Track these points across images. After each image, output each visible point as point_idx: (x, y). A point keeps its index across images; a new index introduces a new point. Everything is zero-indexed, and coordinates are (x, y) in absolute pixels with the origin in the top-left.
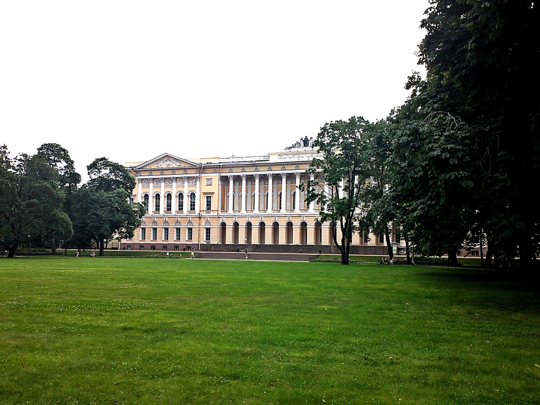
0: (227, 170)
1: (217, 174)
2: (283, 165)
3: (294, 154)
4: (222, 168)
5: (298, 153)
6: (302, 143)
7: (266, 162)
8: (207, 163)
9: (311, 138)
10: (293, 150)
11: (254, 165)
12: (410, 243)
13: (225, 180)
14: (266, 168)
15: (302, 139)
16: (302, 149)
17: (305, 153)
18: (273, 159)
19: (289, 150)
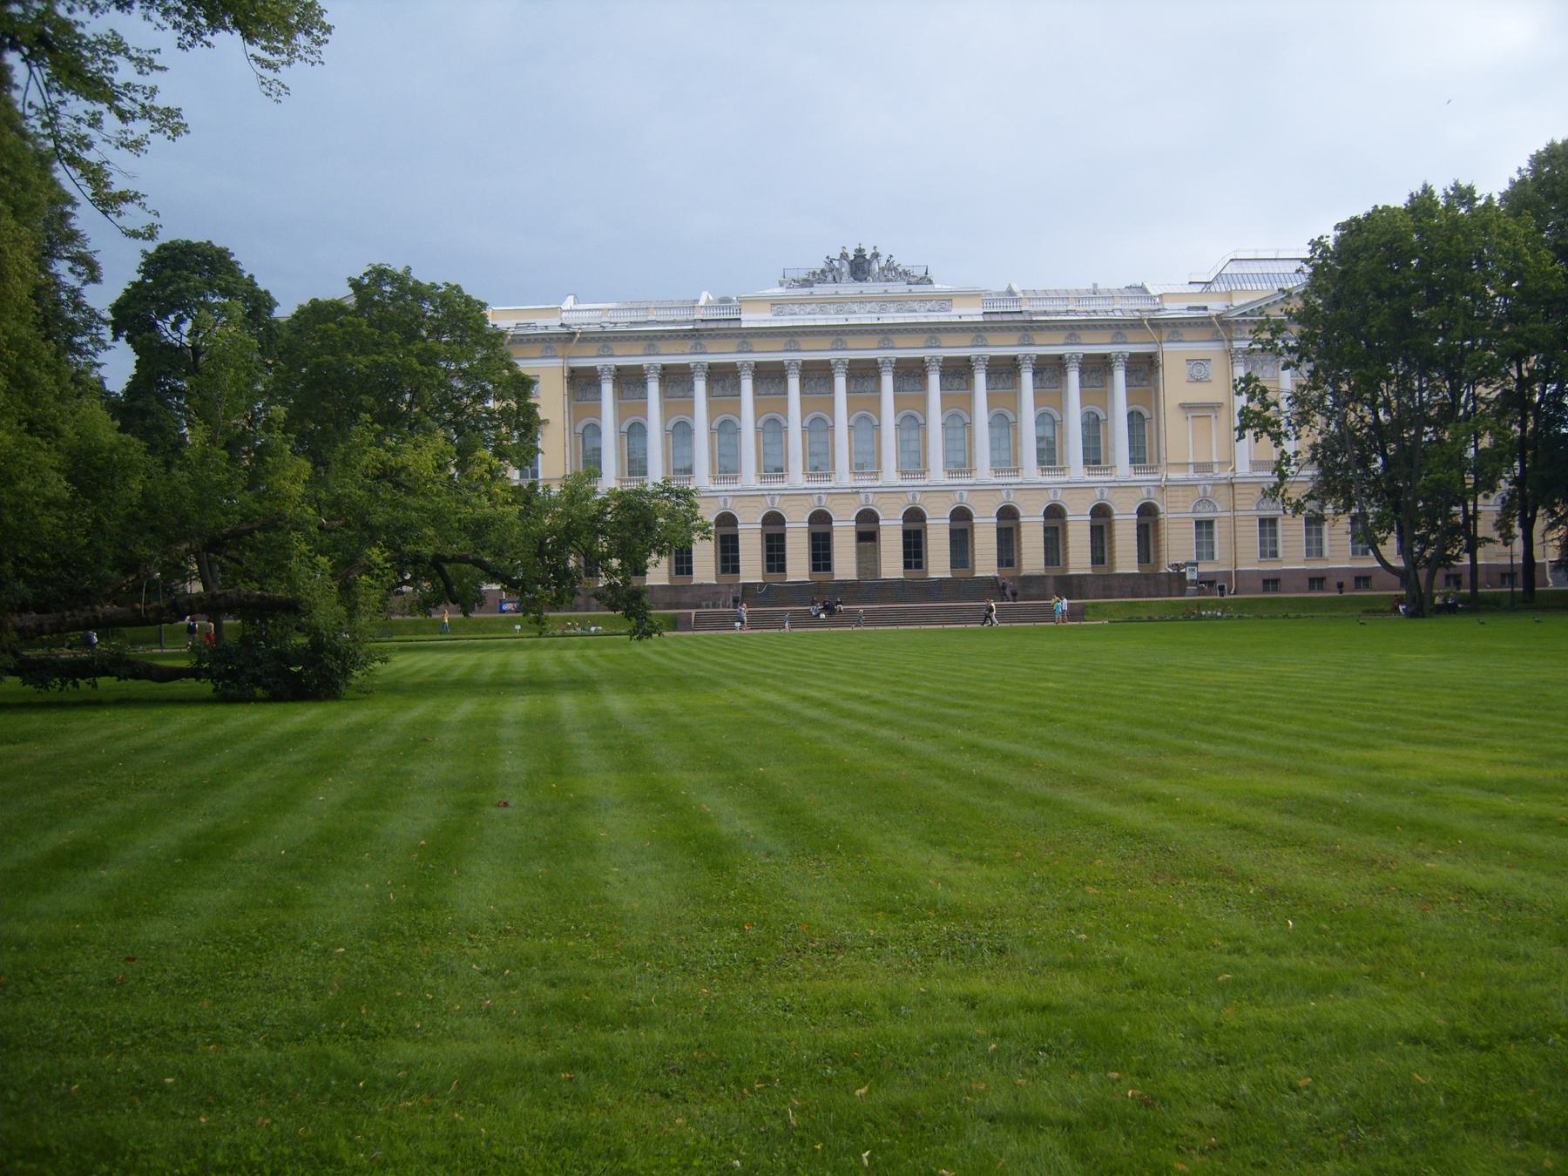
0: (593, 349)
1: (558, 362)
2: (791, 335)
3: (824, 303)
4: (579, 340)
5: (839, 302)
6: (846, 269)
7: (733, 325)
8: (1189, 308)
9: (876, 256)
10: (820, 290)
11: (696, 335)
12: (1466, 561)
13: (582, 382)
14: (732, 344)
15: (844, 256)
16: (849, 288)
17: (862, 300)
18: (753, 319)
19: (805, 291)
